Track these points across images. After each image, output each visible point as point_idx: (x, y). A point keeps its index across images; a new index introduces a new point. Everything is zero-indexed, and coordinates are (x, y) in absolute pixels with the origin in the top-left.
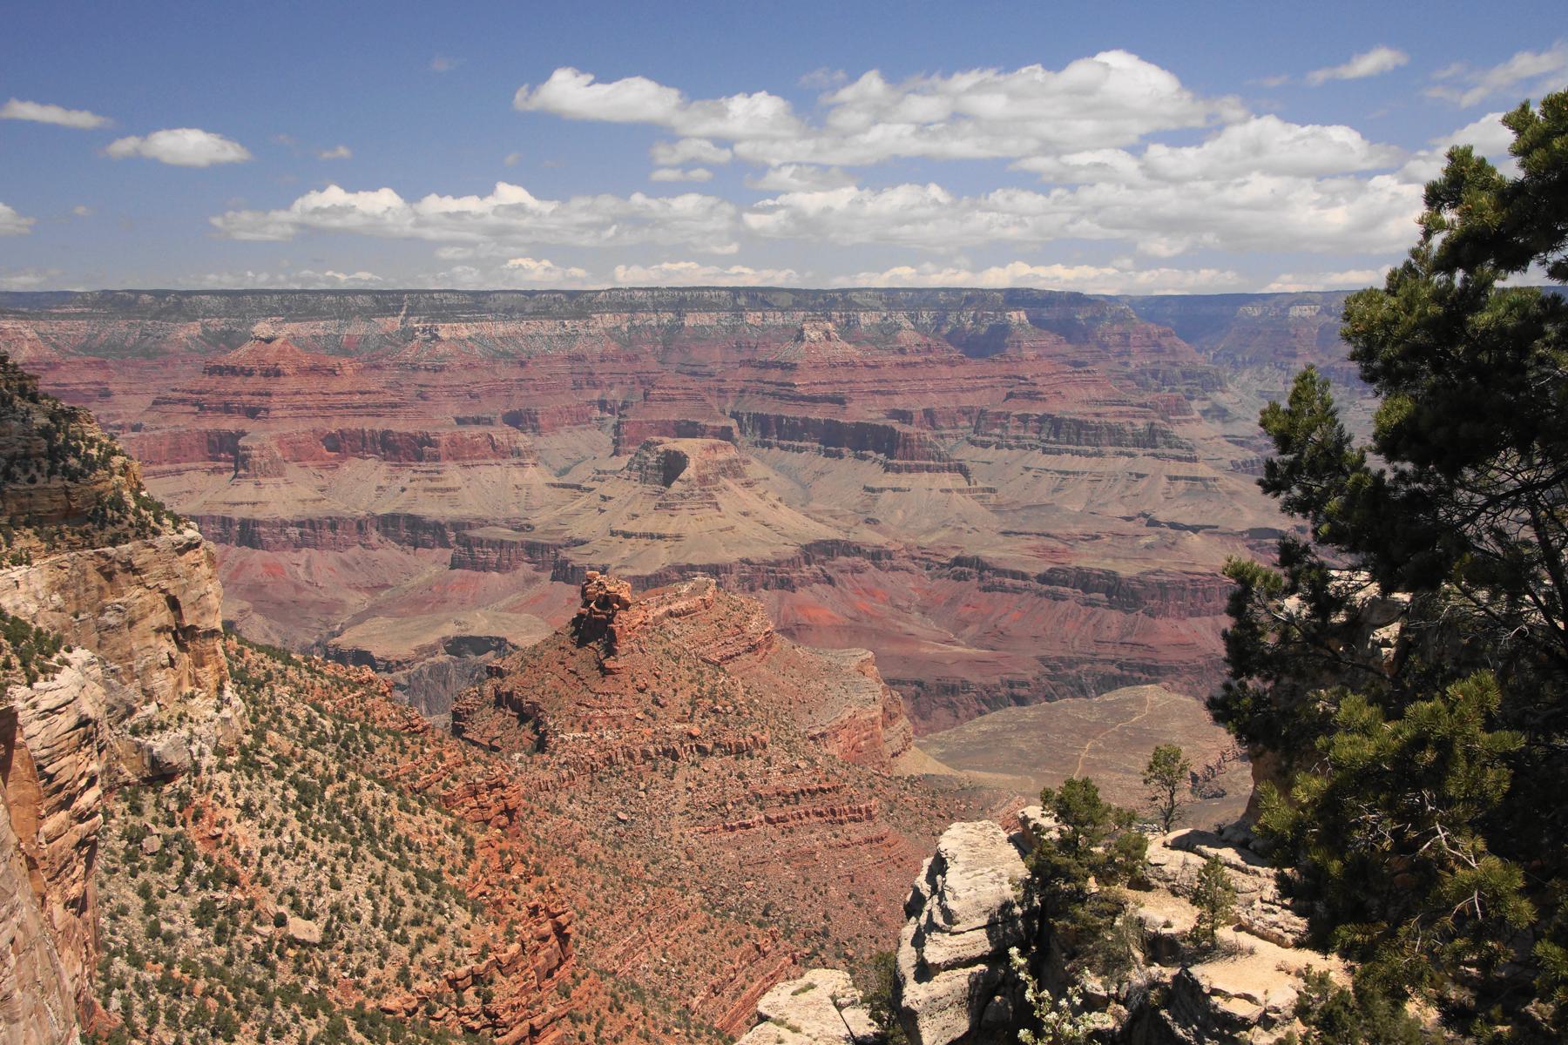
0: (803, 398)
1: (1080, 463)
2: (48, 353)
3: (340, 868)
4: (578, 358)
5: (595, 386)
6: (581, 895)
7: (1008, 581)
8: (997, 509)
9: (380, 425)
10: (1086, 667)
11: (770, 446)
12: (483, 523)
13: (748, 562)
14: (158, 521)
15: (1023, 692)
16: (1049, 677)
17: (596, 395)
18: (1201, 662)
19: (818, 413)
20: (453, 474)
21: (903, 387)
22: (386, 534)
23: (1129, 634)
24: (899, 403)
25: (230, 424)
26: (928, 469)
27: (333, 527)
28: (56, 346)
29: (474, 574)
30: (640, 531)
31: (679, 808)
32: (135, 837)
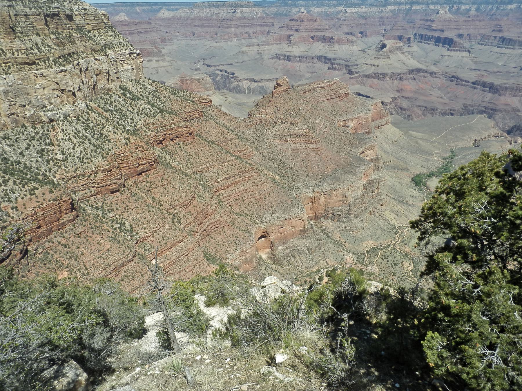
0: (434, 30)
1: (507, 51)
2: (264, 15)
3: (77, 145)
4: (381, 18)
5: (384, 25)
6: (202, 153)
7: (464, 83)
8: (476, 63)
10: (476, 107)
11: (422, 42)
12: (340, 59)
13: (393, 73)
14: (55, 65)
16: (463, 109)
17: (384, 27)
18: (510, 109)
19: (436, 34)
20: (337, 47)
21: (464, 27)
22: (319, 60)
23: (492, 100)
24: (461, 32)
25: (291, 33)
26: (459, 51)
32: (37, 133)
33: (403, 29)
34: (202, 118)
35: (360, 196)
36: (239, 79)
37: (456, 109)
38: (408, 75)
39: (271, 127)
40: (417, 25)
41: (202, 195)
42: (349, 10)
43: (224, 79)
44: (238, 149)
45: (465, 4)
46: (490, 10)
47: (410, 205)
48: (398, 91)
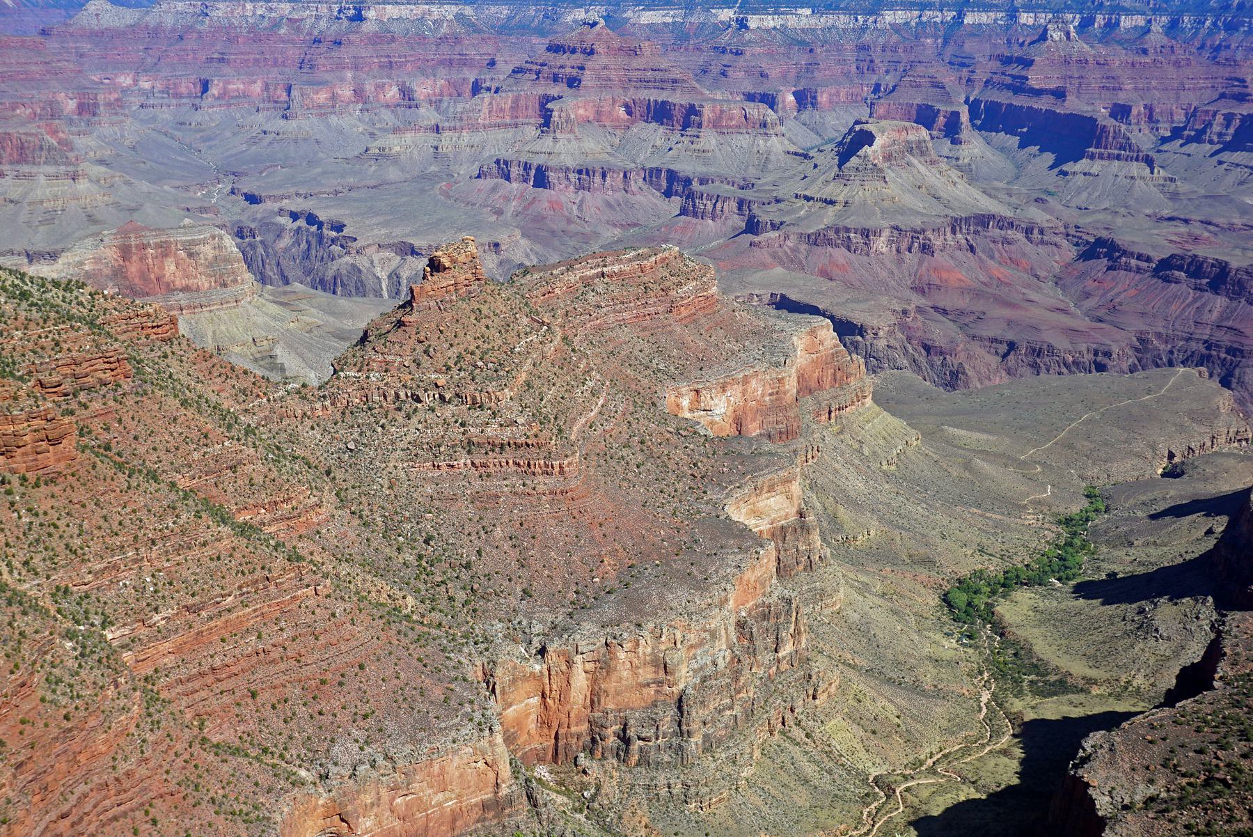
4: (864, 48)
7: (1133, 262)
8: (1174, 196)
9: (662, 96)
10: (1181, 343)
12: (725, 180)
13: (896, 228)
15: (1105, 360)
16: (1137, 350)
19: (1042, 104)
22: (651, 183)
23: (1228, 318)
24: (1122, 98)
25: (554, 90)
26: (1118, 157)
27: (604, 176)
28: (473, 25)
29: (694, 220)
30: (817, 196)
31: (403, 445)
33: (938, 85)
34: (126, 386)
35: (721, 664)
36: (358, 244)
37: (1115, 350)
38: (949, 236)
39: (400, 417)
40: (981, 75)
41: (67, 679)
42: (753, 22)
43: (304, 245)
44: (263, 497)
45: (1129, 12)
46: (1211, 33)
47: (924, 693)
48: (920, 290)
